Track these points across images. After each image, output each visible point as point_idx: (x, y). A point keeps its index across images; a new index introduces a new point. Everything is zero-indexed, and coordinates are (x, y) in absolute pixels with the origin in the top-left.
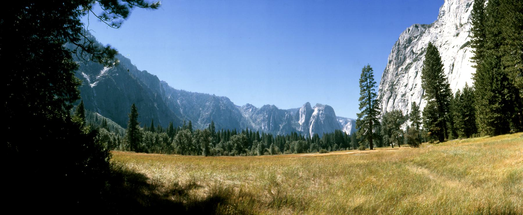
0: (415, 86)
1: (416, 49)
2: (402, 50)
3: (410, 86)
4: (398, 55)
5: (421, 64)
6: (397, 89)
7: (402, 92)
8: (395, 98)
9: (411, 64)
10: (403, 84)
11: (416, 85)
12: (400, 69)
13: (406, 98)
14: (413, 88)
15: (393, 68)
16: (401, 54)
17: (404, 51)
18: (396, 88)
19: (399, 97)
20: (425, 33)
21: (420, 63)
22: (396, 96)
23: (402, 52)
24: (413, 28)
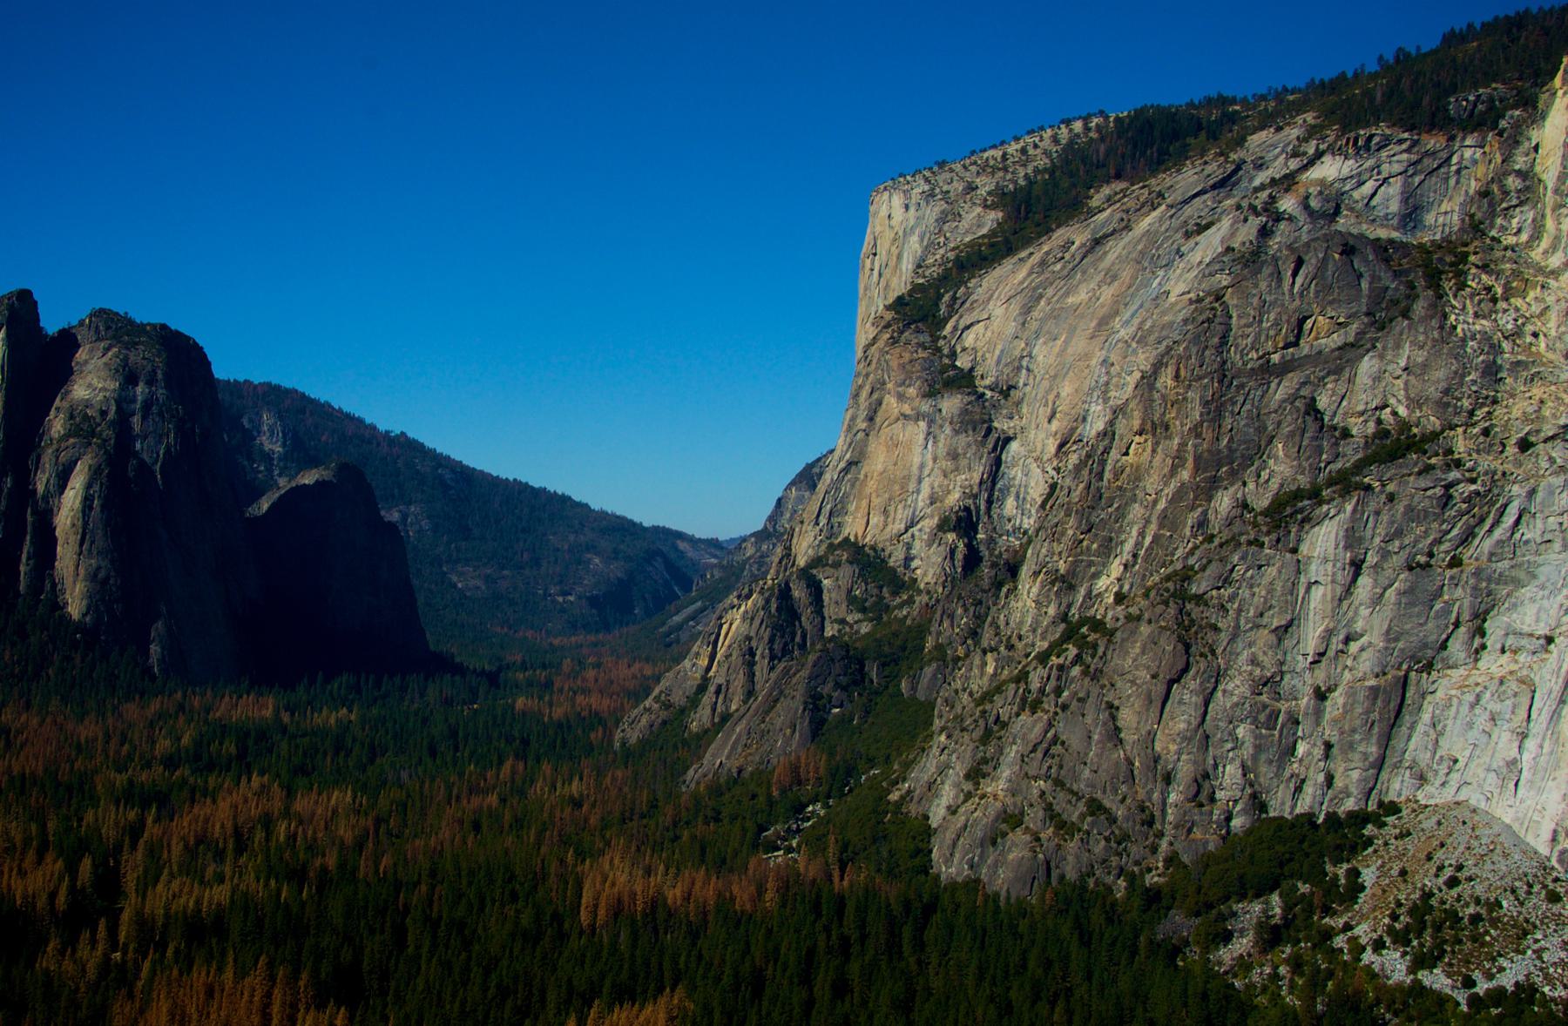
0: (1340, 646)
2: (1241, 386)
3: (1311, 636)
4: (1215, 410)
5: (1385, 518)
6: (1224, 637)
7: (1254, 661)
8: (1210, 686)
9: (1315, 495)
10: (1261, 615)
11: (1348, 640)
12: (1224, 502)
13: (1283, 706)
14: (1331, 653)
15: (1174, 485)
16: (1237, 410)
17: (1259, 393)
18: (1216, 629)
19: (1236, 687)
20: (1405, 314)
21: (1377, 513)
22: (1218, 676)
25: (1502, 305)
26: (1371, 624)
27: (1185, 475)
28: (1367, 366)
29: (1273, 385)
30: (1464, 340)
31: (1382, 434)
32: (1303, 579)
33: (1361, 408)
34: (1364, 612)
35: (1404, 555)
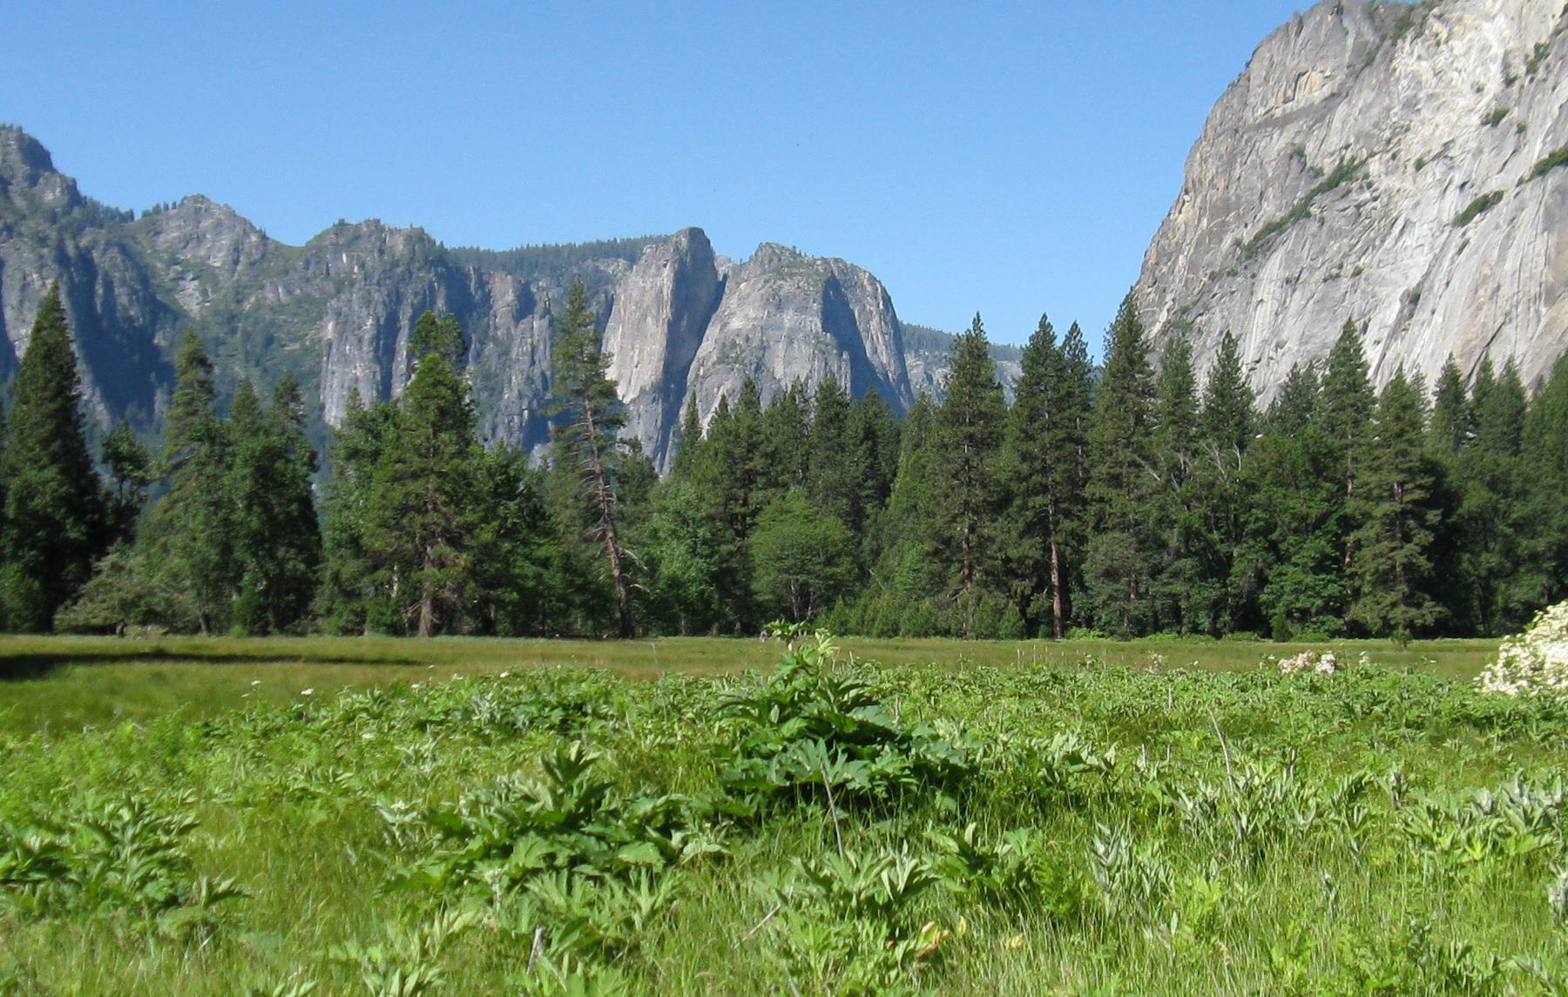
1: (1318, 143)
14: (1264, 361)
23: (1248, 150)
24: (1320, 23)
25: (1443, 47)
26: (1291, 331)
27: (1205, 222)
28: (1341, 110)
29: (1275, 137)
30: (1398, 80)
31: (1340, 167)
32: (1255, 300)
33: (1333, 149)
34: (1290, 322)
35: (1323, 269)
